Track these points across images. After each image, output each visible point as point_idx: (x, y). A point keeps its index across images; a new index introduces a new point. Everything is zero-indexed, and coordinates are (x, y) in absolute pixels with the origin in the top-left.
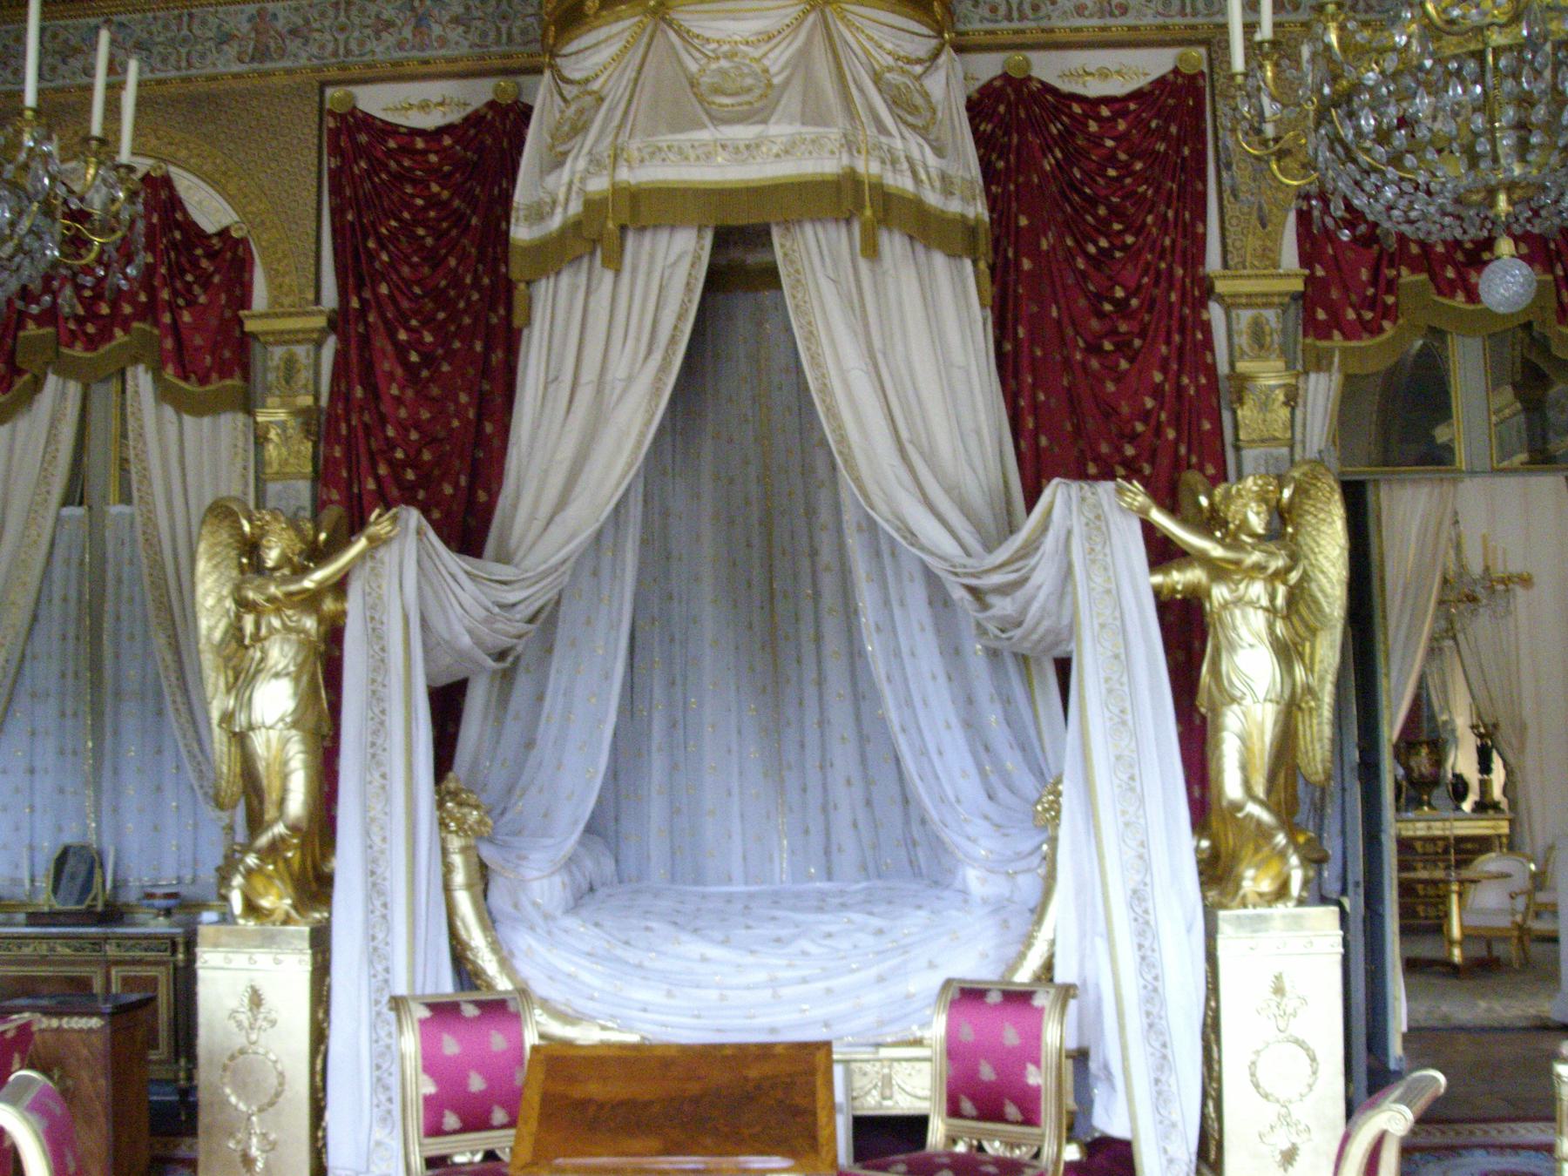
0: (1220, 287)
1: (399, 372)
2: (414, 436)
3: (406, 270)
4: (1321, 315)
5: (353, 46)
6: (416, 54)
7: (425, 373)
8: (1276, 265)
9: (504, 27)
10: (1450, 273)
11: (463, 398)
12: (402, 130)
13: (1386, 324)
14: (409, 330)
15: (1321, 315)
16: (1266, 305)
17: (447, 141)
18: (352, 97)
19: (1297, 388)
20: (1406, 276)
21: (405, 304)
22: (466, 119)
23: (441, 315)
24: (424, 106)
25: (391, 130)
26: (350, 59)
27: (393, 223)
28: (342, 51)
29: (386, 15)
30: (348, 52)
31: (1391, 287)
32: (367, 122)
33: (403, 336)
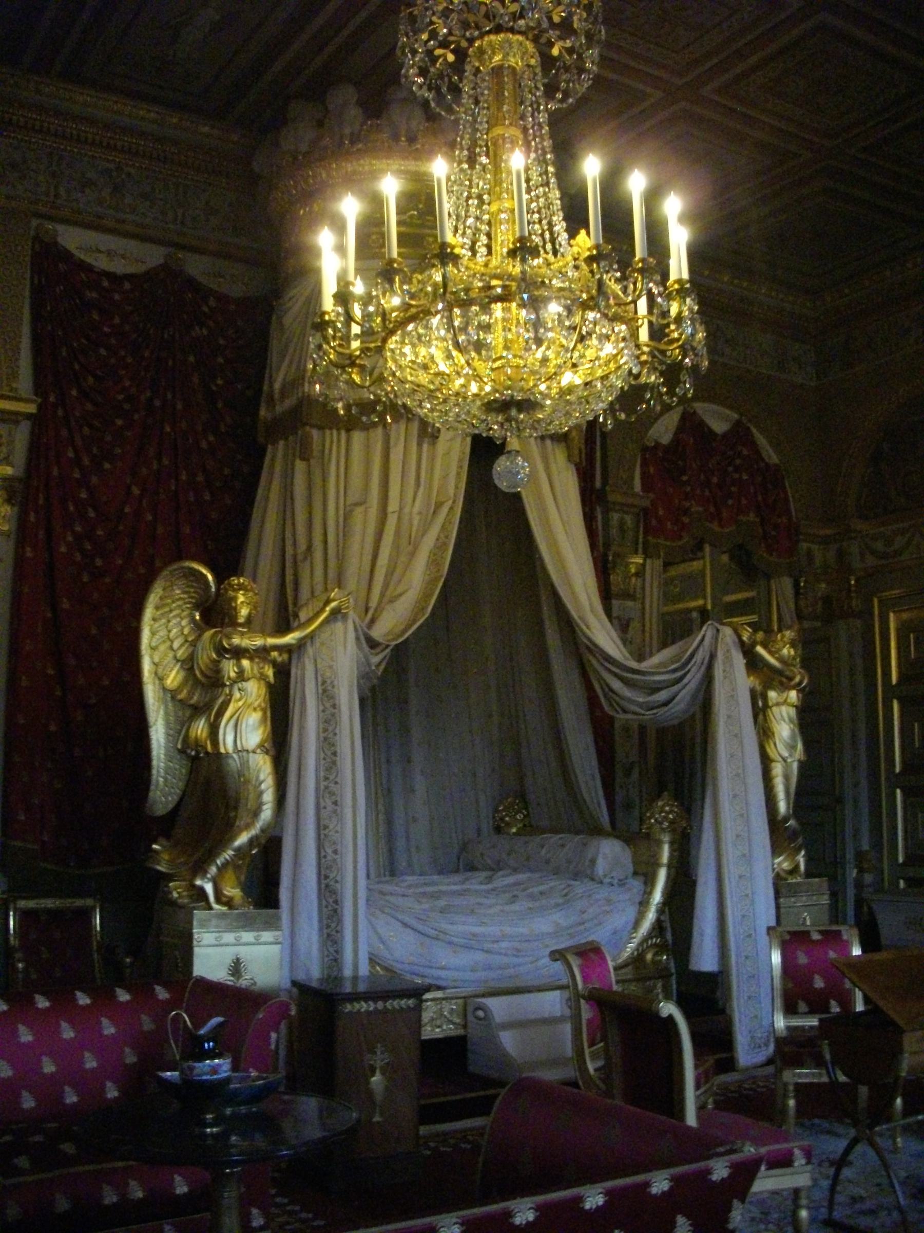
0: (612, 497)
1: (86, 461)
2: (92, 514)
3: (91, 380)
4: (654, 522)
5: (62, 191)
6: (111, 212)
7: (107, 466)
8: (632, 487)
9: (180, 212)
10: (712, 509)
11: (136, 491)
12: (96, 270)
13: (683, 534)
14: (91, 426)
15: (654, 522)
16: (627, 513)
17: (127, 285)
18: (55, 230)
19: (644, 565)
20: (696, 508)
21: (89, 407)
22: (147, 273)
23: (119, 422)
24: (110, 254)
25: (89, 269)
26: (59, 201)
27: (84, 341)
28: (52, 193)
29: (89, 175)
30: (57, 196)
31: (686, 512)
32: (67, 256)
33: (86, 430)
